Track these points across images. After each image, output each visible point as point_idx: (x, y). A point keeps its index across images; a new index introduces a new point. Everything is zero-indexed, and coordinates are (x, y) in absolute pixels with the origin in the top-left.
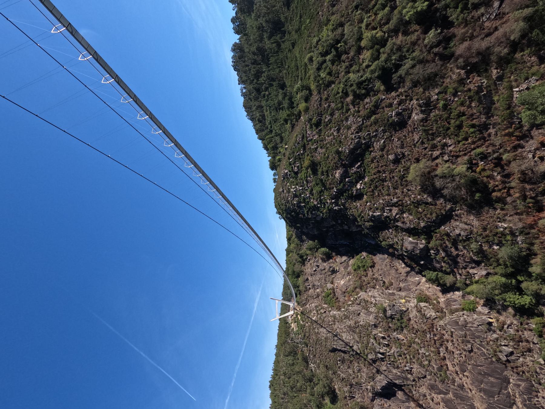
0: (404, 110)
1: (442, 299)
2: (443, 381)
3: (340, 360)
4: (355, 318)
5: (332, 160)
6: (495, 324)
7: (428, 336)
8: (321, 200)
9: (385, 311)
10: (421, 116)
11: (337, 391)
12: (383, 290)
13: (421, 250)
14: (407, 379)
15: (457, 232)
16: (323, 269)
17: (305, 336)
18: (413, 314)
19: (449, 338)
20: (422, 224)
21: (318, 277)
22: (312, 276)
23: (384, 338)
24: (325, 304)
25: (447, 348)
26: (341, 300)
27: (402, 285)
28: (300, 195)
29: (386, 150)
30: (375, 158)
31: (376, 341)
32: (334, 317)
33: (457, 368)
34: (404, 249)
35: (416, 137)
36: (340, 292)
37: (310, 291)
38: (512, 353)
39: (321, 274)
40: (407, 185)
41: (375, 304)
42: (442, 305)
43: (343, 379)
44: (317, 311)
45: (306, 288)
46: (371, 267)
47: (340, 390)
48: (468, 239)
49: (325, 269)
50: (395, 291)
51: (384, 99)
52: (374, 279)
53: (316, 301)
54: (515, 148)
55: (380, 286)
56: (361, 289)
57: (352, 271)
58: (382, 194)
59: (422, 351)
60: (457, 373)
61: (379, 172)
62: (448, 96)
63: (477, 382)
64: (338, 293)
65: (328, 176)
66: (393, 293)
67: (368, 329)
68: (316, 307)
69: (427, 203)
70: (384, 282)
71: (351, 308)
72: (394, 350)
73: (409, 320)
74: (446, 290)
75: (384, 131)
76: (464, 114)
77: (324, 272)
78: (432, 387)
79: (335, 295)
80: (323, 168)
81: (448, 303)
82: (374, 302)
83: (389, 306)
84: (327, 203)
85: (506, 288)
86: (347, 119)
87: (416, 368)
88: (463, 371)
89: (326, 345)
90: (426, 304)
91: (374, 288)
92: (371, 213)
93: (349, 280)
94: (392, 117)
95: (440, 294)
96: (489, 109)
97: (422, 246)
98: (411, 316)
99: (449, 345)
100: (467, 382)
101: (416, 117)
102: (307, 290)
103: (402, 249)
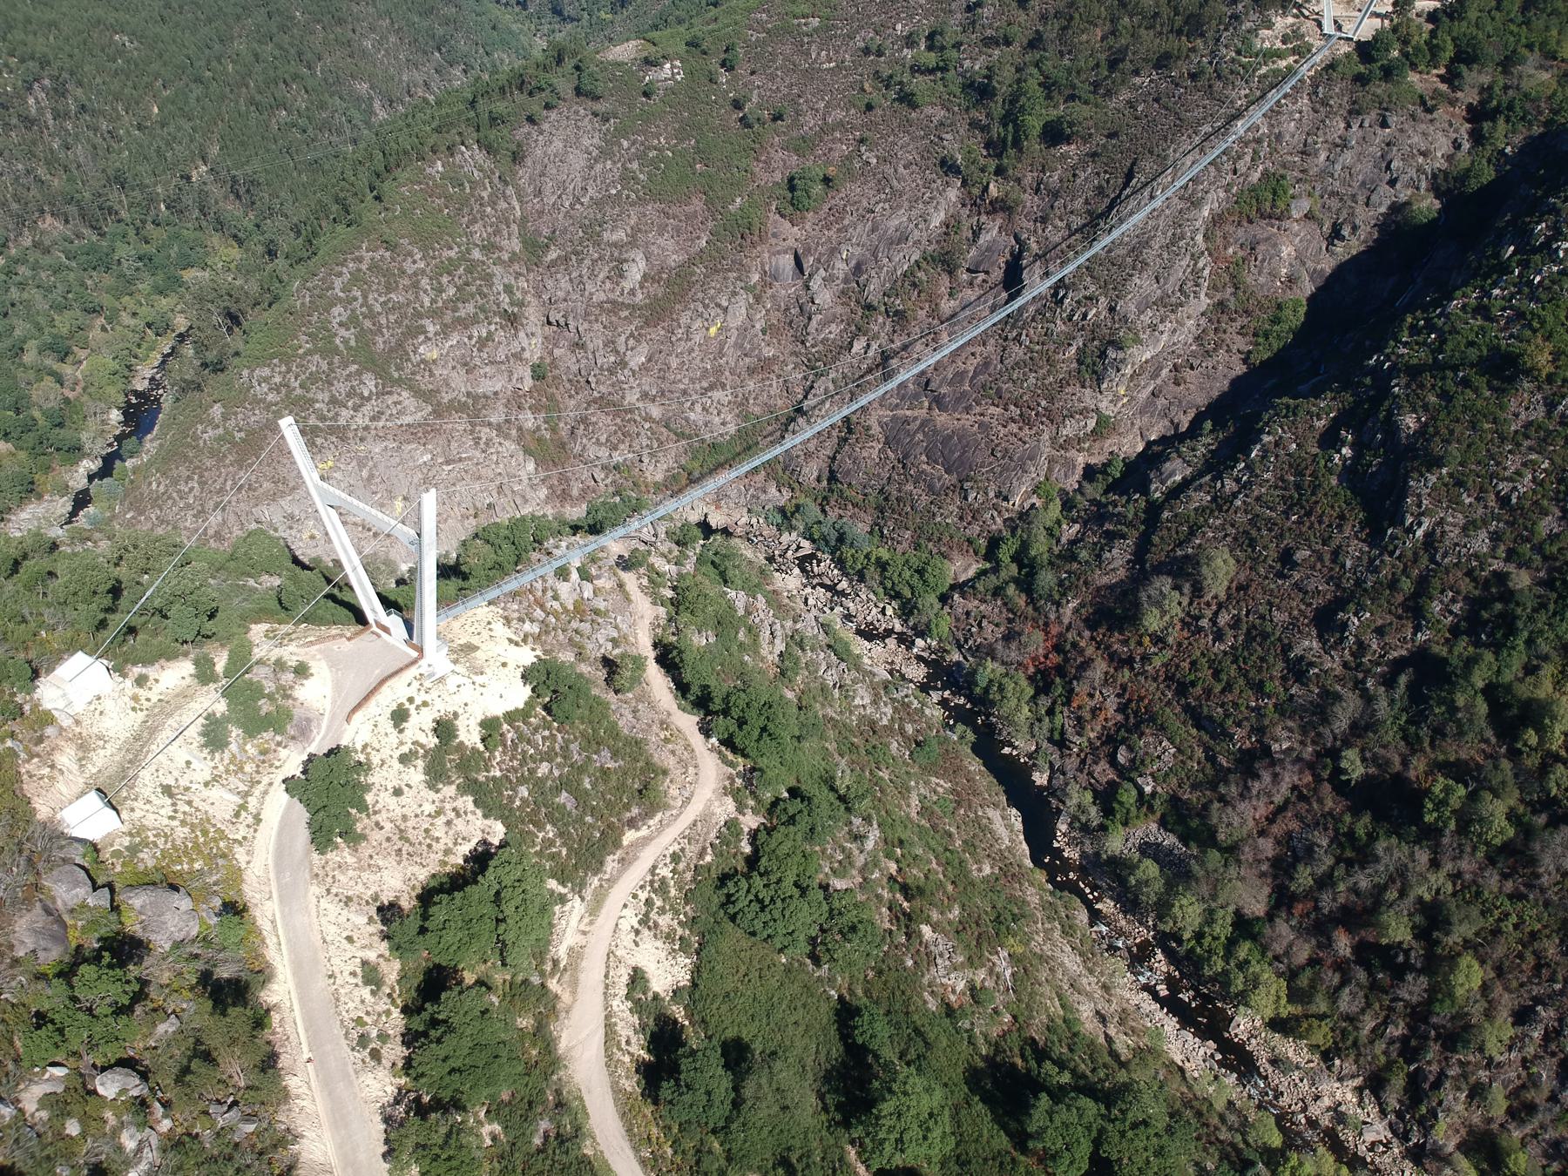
0: (1342, 639)
1: (1081, 460)
2: (983, 386)
3: (1108, 182)
4: (1155, 265)
5: (1452, 432)
6: (1005, 504)
7: (1043, 403)
8: (1430, 327)
9: (1119, 347)
10: (1297, 652)
11: (1065, 148)
12: (1179, 356)
13: (1151, 481)
14: (1013, 327)
15: (1115, 551)
16: (1374, 198)
17: (1219, 77)
18: (1088, 397)
19: (1022, 434)
20: (1166, 514)
21: (1365, 169)
22: (1388, 144)
23: (1085, 316)
24: (1265, 174)
25: (1014, 421)
26: (1240, 232)
27: (1161, 402)
28: (1525, 265)
29: (1327, 557)
30: (1340, 527)
31: (1086, 298)
32: (1196, 204)
33: (987, 419)
34: (1174, 455)
35: (1279, 617)
36: (1261, 234)
37: (1342, 125)
38: (966, 498)
39: (1363, 184)
40: (1235, 539)
41: (1153, 327)
42: (1072, 453)
43: (1074, 175)
44: (1258, 141)
45: (1358, 113)
46: (1250, 352)
47: (1064, 157)
48: (1099, 556)
49: (1367, 205)
50: (1159, 381)
51: (1415, 634)
52: (1217, 346)
53: (1299, 138)
54: (1124, 688)
55: (1193, 355)
56: (1221, 306)
57: (1289, 295)
58: (1276, 487)
59: (1032, 380)
60: (982, 415)
61: (1308, 514)
62: (1270, 703)
63: (962, 435)
64: (1262, 229)
65: (1445, 396)
66: (1158, 376)
67: (1115, 289)
68: (1279, 137)
69: (1180, 544)
70: (1192, 368)
71: (1184, 263)
72: (1060, 327)
73: (1083, 387)
74: (1090, 473)
75: (1359, 583)
76: (1223, 691)
77: (1361, 199)
78: (986, 364)
79: (1262, 217)
80: (1476, 390)
81: (1070, 465)
82: (1161, 327)
83: (1123, 361)
84: (1405, 344)
85: (1025, 546)
86: (1496, 538)
87: (1017, 352)
88: (981, 425)
89: (1151, 152)
90: (1090, 428)
91: (1197, 338)
92: (1266, 439)
93: (1274, 275)
94: (1356, 614)
95: (1093, 461)
96: (1193, 717)
97: (1153, 487)
98: (1088, 391)
99: (1013, 427)
100: (968, 420)
101: (1309, 644)
102: (1355, 111)
103: (1178, 451)
